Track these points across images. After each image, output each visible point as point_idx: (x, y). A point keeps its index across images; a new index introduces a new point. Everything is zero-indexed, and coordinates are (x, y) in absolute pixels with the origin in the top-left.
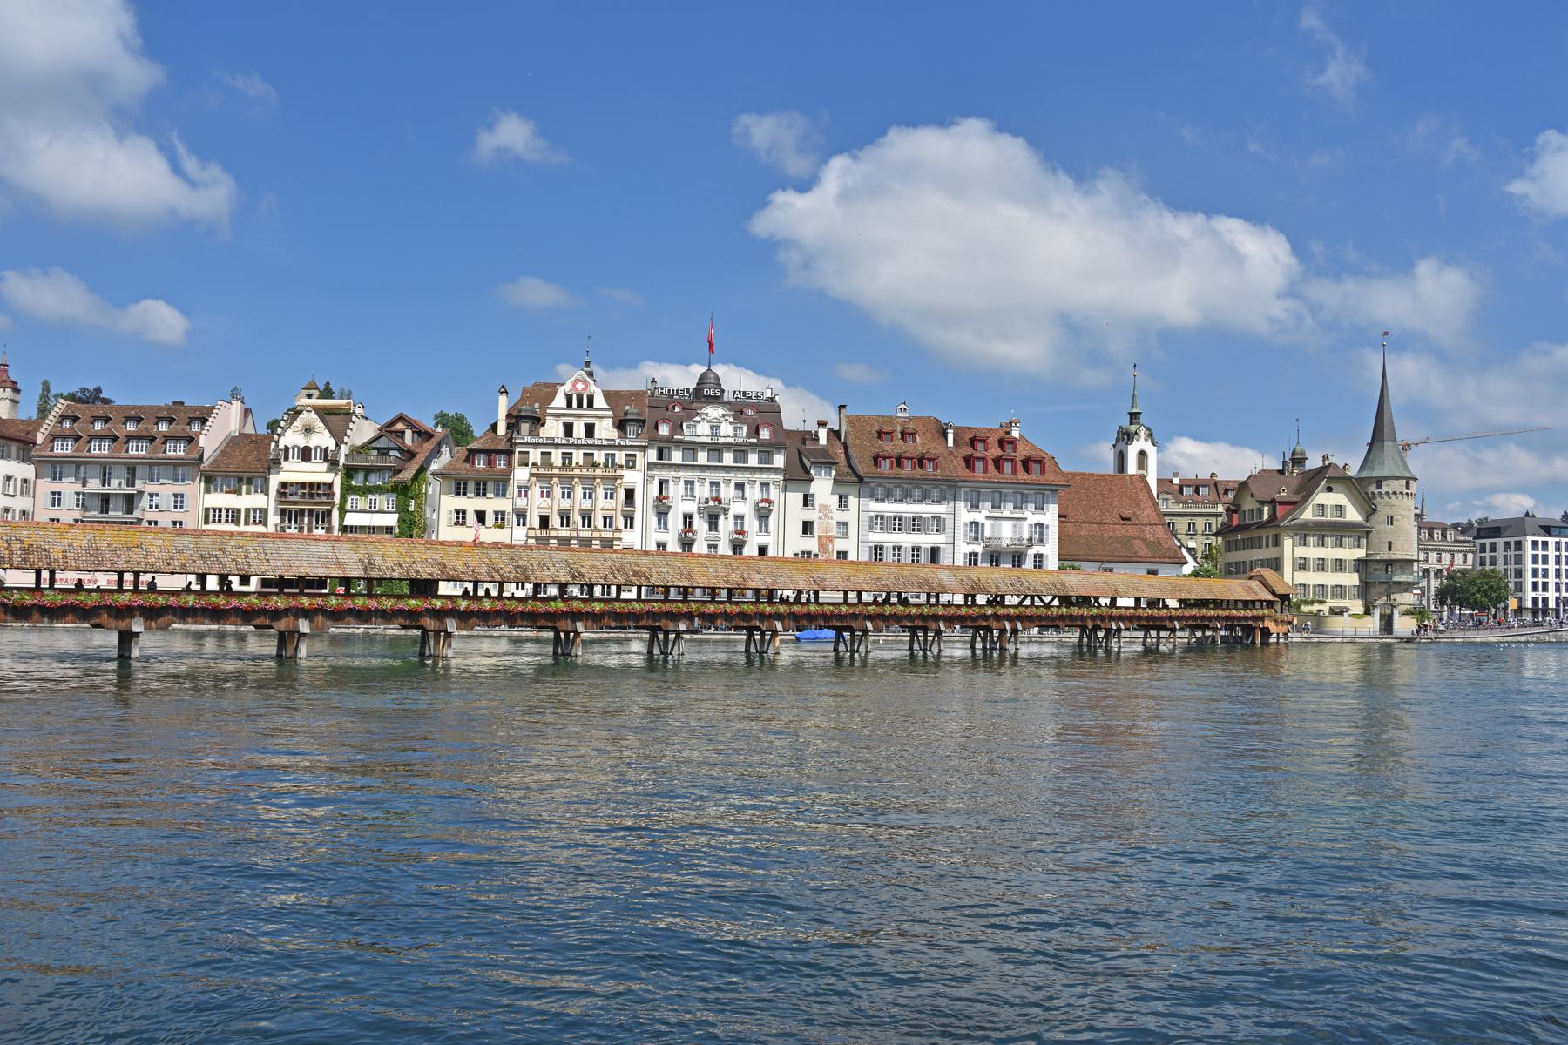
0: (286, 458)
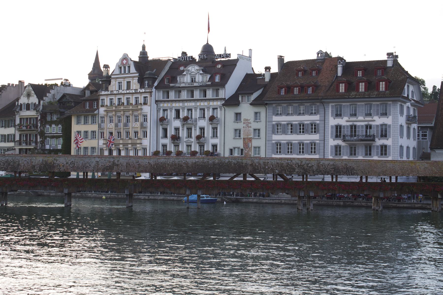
0: (21, 109)
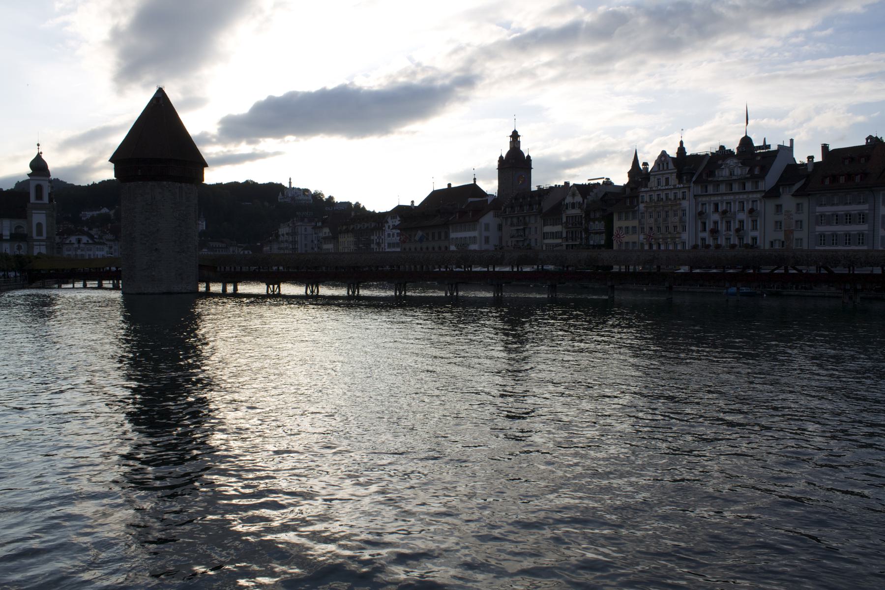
0: (567, 208)
